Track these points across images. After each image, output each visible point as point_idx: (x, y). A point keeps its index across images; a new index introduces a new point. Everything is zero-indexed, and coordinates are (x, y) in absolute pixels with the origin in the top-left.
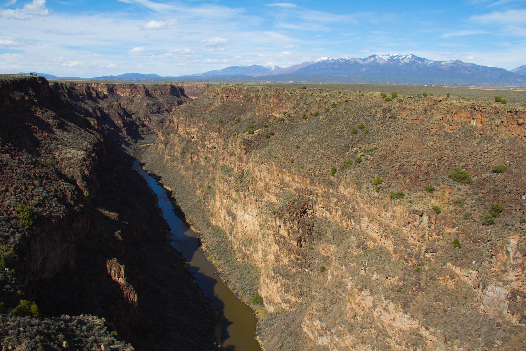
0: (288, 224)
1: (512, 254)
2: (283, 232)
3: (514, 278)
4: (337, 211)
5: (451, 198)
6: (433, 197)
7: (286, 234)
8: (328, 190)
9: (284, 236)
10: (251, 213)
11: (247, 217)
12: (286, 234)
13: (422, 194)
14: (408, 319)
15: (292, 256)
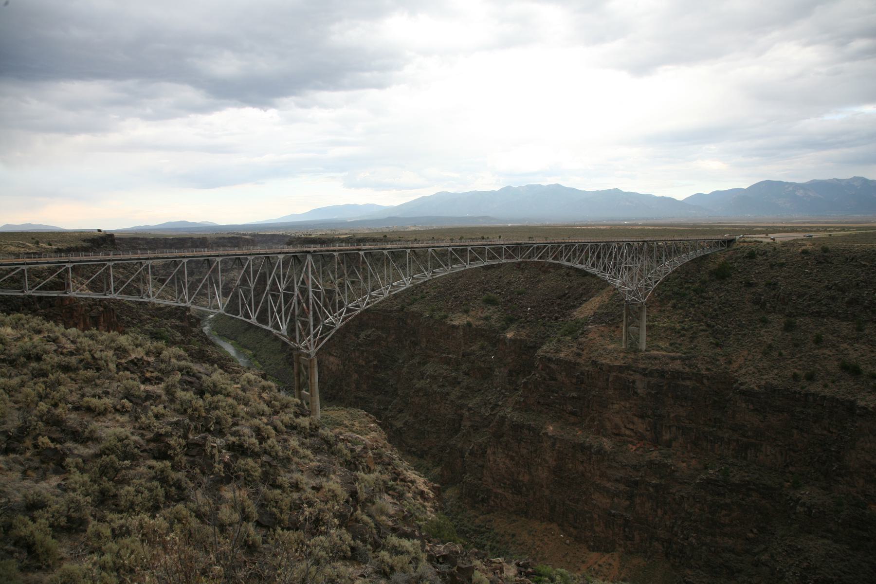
0: (365, 354)
1: (508, 344)
2: (362, 362)
3: (511, 361)
4: (406, 340)
5: (482, 316)
6: (469, 316)
7: (364, 363)
8: (399, 323)
9: (362, 365)
10: (335, 354)
11: (332, 359)
12: (364, 363)
13: (461, 314)
14: (450, 404)
15: (370, 381)
